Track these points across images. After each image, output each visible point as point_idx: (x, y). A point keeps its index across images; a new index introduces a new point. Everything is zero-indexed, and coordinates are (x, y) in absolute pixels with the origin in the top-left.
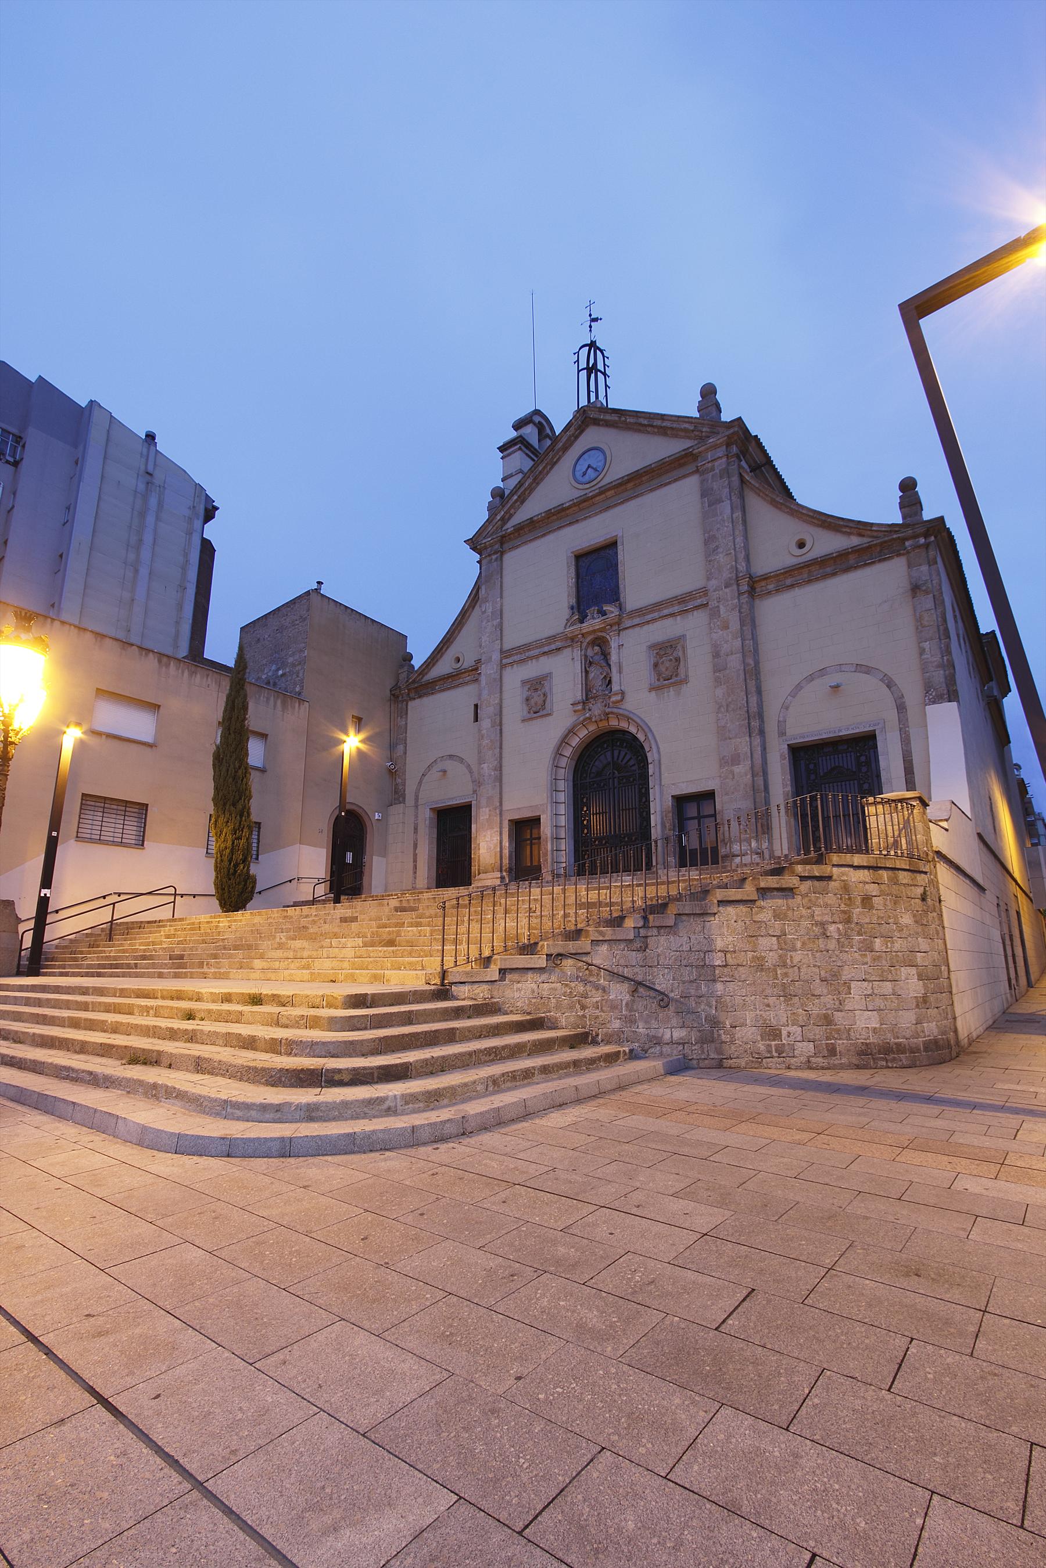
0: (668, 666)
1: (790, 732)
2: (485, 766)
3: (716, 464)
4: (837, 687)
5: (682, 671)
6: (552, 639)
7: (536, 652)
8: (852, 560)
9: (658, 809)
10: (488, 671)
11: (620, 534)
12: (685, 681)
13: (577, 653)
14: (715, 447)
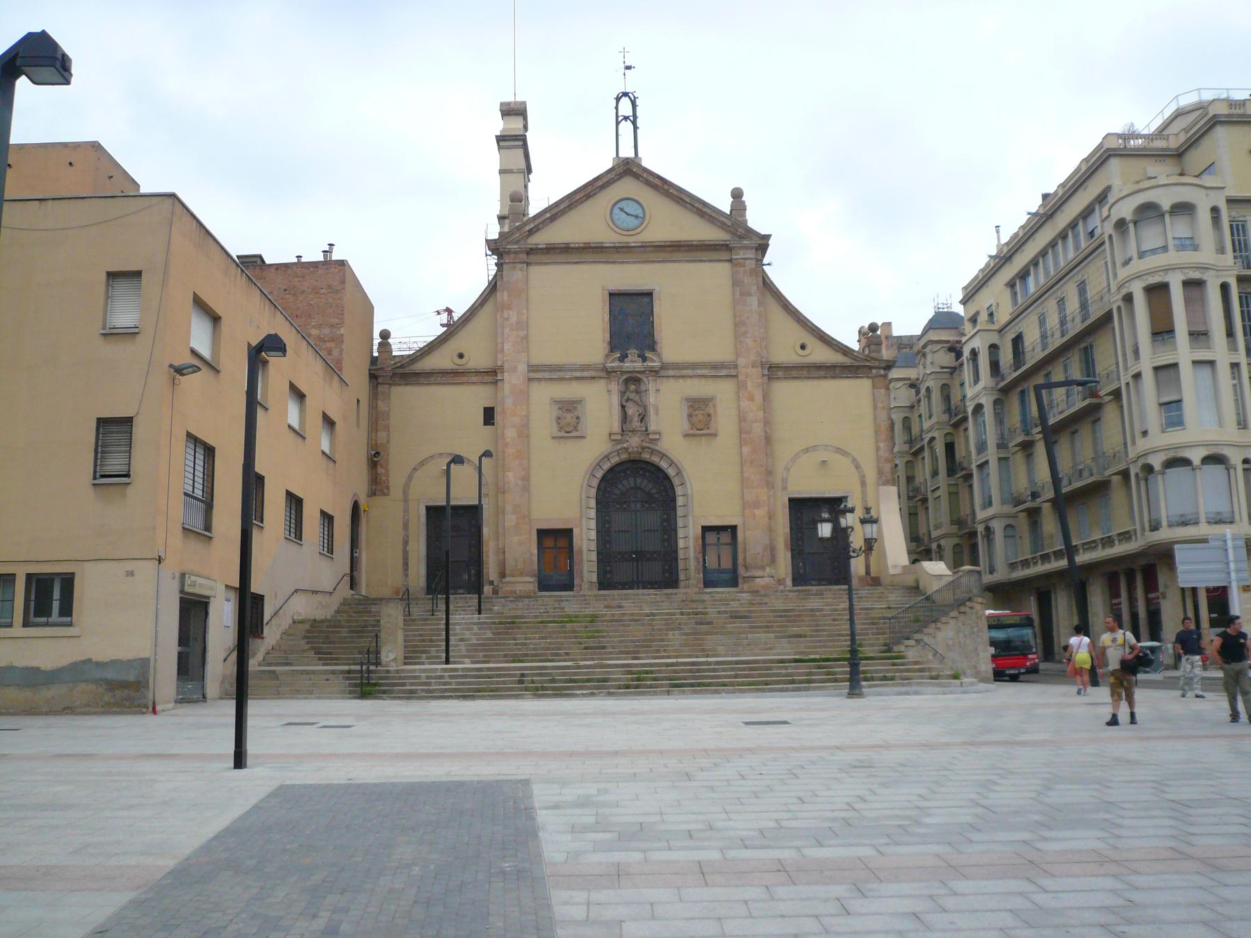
0: (700, 417)
1: (790, 488)
3: (747, 262)
4: (824, 462)
5: (712, 424)
6: (585, 368)
8: (837, 371)
9: (691, 535)
10: (512, 379)
11: (657, 290)
12: (714, 435)
13: (615, 387)
14: (746, 248)
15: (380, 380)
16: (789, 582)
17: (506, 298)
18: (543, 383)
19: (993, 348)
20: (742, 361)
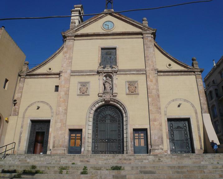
0: (132, 89)
2: (61, 108)
3: (149, 38)
7: (85, 74)
11: (118, 47)
14: (148, 34)
15: (22, 77)
16: (169, 152)
17: (66, 50)
18: (76, 76)
19: (216, 90)
20: (147, 69)
